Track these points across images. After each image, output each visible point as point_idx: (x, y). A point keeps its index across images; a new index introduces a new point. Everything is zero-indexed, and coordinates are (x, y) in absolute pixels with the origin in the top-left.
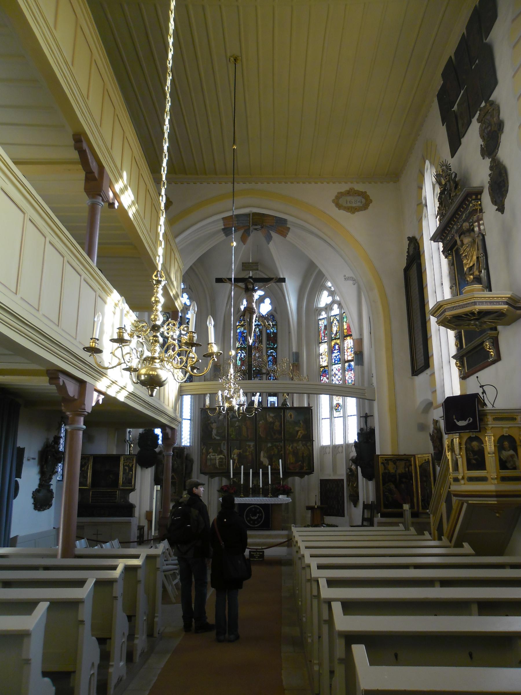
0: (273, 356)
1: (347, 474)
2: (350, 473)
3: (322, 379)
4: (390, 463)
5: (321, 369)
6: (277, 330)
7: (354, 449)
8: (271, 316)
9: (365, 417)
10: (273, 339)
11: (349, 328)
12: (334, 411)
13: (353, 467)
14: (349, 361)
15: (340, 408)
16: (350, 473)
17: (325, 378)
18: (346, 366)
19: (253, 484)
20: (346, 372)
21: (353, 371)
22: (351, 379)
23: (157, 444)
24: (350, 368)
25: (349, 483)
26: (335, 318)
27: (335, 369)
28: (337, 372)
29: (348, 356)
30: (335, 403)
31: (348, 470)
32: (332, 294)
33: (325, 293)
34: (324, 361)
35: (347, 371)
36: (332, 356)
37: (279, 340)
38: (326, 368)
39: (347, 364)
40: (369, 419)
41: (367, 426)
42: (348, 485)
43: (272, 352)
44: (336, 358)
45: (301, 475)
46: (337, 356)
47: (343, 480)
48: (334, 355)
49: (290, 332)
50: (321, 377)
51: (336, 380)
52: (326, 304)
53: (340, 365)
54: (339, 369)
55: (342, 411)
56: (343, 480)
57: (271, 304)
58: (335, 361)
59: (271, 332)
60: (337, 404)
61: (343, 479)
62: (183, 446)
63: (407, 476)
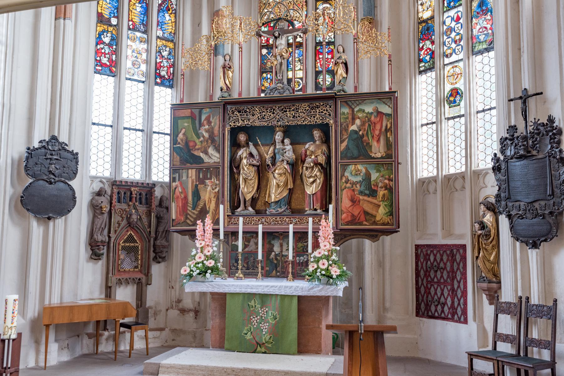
1: (473, 235)
2: (480, 232)
3: (421, 47)
5: (421, 27)
9: (521, 98)
12: (447, 106)
13: (488, 218)
15: (458, 98)
16: (480, 232)
17: (428, 43)
18: (473, 8)
19: (273, 253)
20: (474, 19)
22: (485, 32)
25: (479, 254)
27: (450, 18)
30: (448, 88)
31: (477, 226)
34: (426, 9)
38: (430, 22)
40: (532, 102)
41: (525, 119)
47: (464, 247)
50: (419, 43)
51: (450, 42)
53: (460, 9)
55: (462, 104)
56: (464, 247)
60: (452, 90)
61: (465, 245)
62: (155, 181)
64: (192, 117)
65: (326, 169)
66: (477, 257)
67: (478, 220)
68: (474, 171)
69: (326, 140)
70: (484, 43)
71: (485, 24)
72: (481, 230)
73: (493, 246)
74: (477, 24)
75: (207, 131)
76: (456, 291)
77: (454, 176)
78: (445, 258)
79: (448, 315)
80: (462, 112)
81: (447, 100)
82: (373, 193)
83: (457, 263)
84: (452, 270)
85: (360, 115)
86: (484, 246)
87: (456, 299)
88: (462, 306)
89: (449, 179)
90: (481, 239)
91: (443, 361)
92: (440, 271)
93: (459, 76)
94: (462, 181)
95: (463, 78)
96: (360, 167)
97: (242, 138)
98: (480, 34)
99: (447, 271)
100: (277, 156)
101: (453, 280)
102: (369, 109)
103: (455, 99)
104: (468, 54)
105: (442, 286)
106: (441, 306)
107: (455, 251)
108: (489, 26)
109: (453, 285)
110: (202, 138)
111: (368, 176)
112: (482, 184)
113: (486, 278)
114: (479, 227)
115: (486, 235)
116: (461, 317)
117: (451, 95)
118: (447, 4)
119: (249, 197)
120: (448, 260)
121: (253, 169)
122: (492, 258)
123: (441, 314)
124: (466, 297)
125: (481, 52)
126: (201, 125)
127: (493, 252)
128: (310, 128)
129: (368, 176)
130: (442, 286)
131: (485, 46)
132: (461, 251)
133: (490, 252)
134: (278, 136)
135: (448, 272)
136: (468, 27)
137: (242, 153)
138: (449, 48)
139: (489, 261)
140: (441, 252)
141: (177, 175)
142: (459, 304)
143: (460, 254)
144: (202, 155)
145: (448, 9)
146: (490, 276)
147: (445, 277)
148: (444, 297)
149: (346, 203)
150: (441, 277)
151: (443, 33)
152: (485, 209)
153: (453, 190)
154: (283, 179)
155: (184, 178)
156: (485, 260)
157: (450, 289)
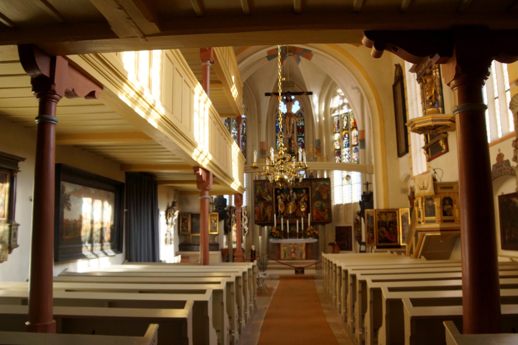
0: (302, 142)
4: (383, 214)
6: (304, 123)
7: (359, 206)
8: (300, 114)
10: (301, 130)
11: (355, 123)
14: (355, 146)
23: (226, 205)
26: (345, 115)
28: (347, 153)
29: (354, 142)
31: (355, 220)
32: (343, 98)
33: (337, 98)
37: (306, 131)
40: (369, 186)
42: (355, 230)
43: (301, 140)
45: (323, 224)
48: (345, 141)
49: (313, 125)
52: (339, 105)
56: (351, 227)
57: (300, 105)
58: (346, 145)
59: (300, 125)
63: (394, 223)
64: (261, 185)
65: (308, 203)
69: (307, 192)
75: (267, 189)
80: (350, 183)
82: (324, 211)
85: (319, 185)
96: (320, 202)
97: (278, 192)
100: (291, 198)
102: (322, 183)
110: (265, 192)
111: (322, 206)
119: (282, 212)
121: (283, 203)
126: (265, 187)
128: (302, 189)
129: (322, 206)
134: (291, 191)
137: (279, 197)
141: (257, 205)
144: (265, 198)
149: (315, 214)
154: (293, 206)
155: (259, 206)
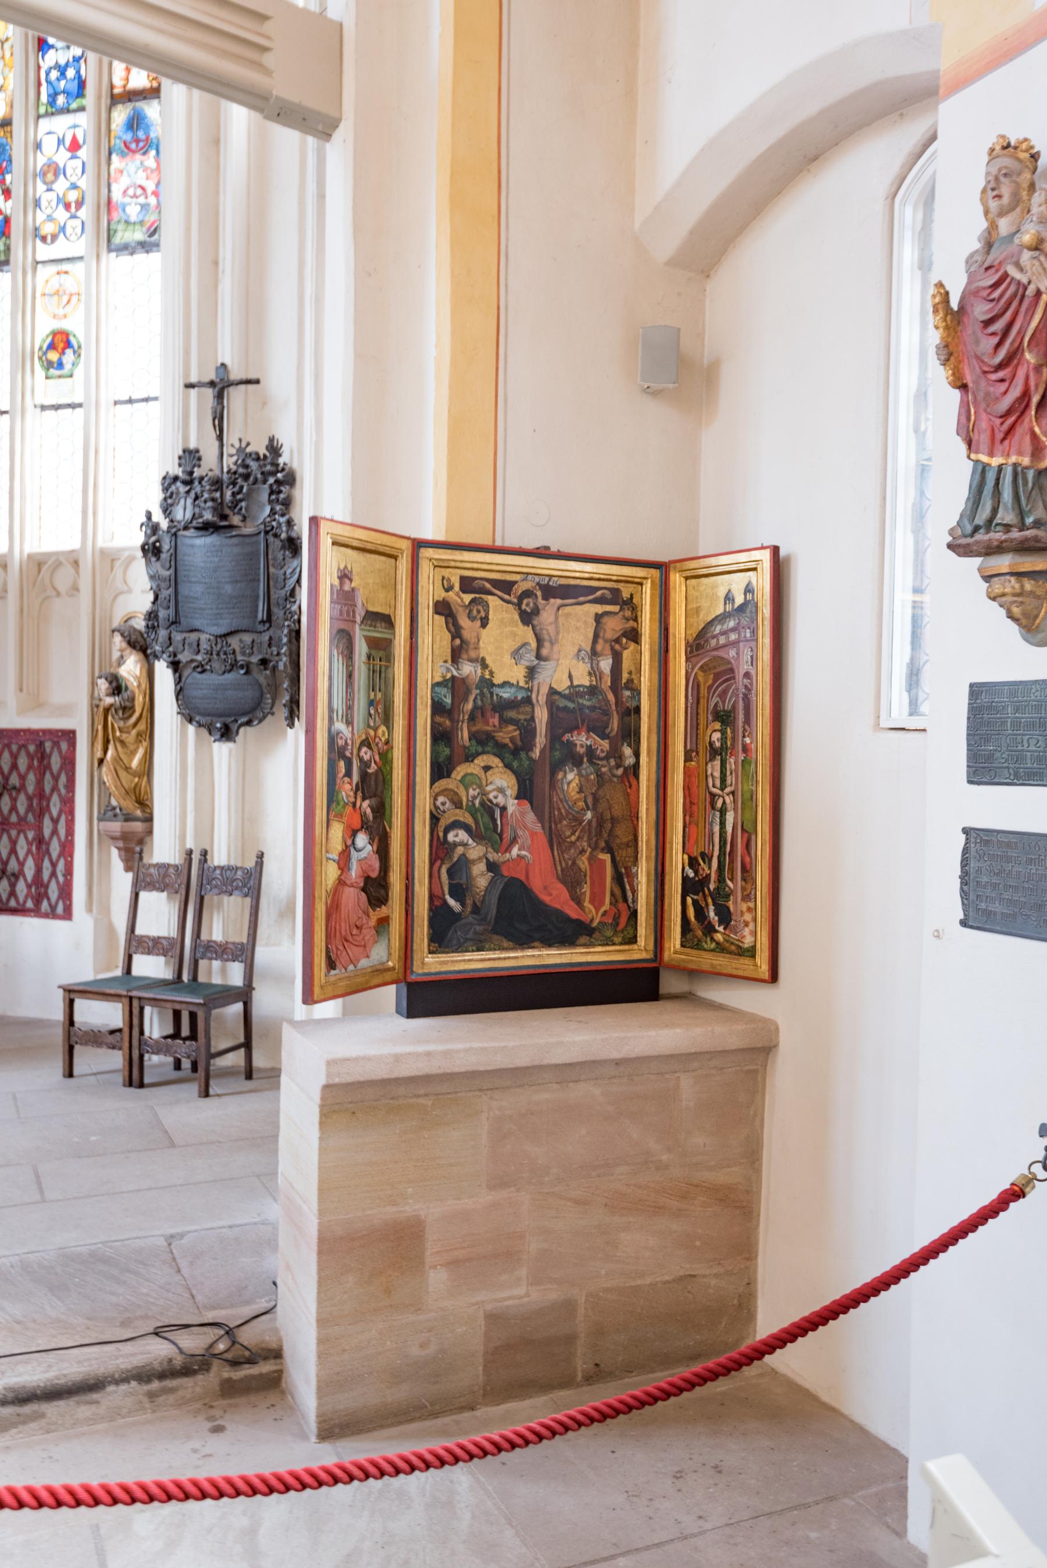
2: (109, 700)
12: (40, 372)
13: (131, 668)
15: (69, 357)
16: (109, 700)
18: (113, 126)
20: (114, 157)
21: (153, 153)
22: (142, 200)
24: (141, 134)
27: (53, 139)
28: (62, 157)
31: (103, 685)
35: (123, 155)
36: (39, 68)
39: (120, 115)
44: (63, 74)
46: (67, 65)
47: (70, 736)
51: (54, 203)
53: (81, 118)
54: (74, 139)
55: (79, 372)
56: (70, 736)
58: (53, 97)
60: (55, 334)
66: (101, 761)
67: (108, 670)
68: (103, 552)
70: (137, 227)
71: (141, 178)
72: (113, 694)
73: (139, 735)
74: (121, 172)
76: (48, 844)
77: (53, 559)
78: (23, 762)
79: (25, 902)
81: (40, 358)
83: (52, 774)
84: (41, 795)
86: (118, 734)
87: (46, 863)
88: (61, 879)
89: (40, 565)
90: (113, 717)
91: (10, 1013)
92: (10, 796)
93: (74, 299)
94: (72, 571)
95: (82, 305)
98: (127, 200)
99: (27, 794)
101: (40, 815)
103: (60, 359)
104: (98, 245)
105: (14, 833)
106: (9, 880)
107: (48, 745)
108: (150, 186)
109: (39, 829)
112: (119, 585)
113: (121, 809)
114: (107, 689)
115: (124, 709)
116: (57, 903)
117: (52, 346)
118: (49, 96)
120: (30, 767)
122: (135, 763)
123: (8, 900)
124: (71, 855)
125: (126, 249)
127: (138, 748)
130: (14, 833)
131: (139, 235)
132: (64, 746)
133: (132, 747)
135: (30, 798)
136: (99, 175)
138: (50, 218)
139: (127, 769)
140: (14, 748)
142: (53, 874)
143: (60, 752)
145: (50, 110)
146: (129, 805)
147: (22, 808)
148: (17, 858)
150: (10, 812)
151: (35, 175)
152: (124, 645)
153: (50, 592)
156: (118, 768)
157: (34, 839)
